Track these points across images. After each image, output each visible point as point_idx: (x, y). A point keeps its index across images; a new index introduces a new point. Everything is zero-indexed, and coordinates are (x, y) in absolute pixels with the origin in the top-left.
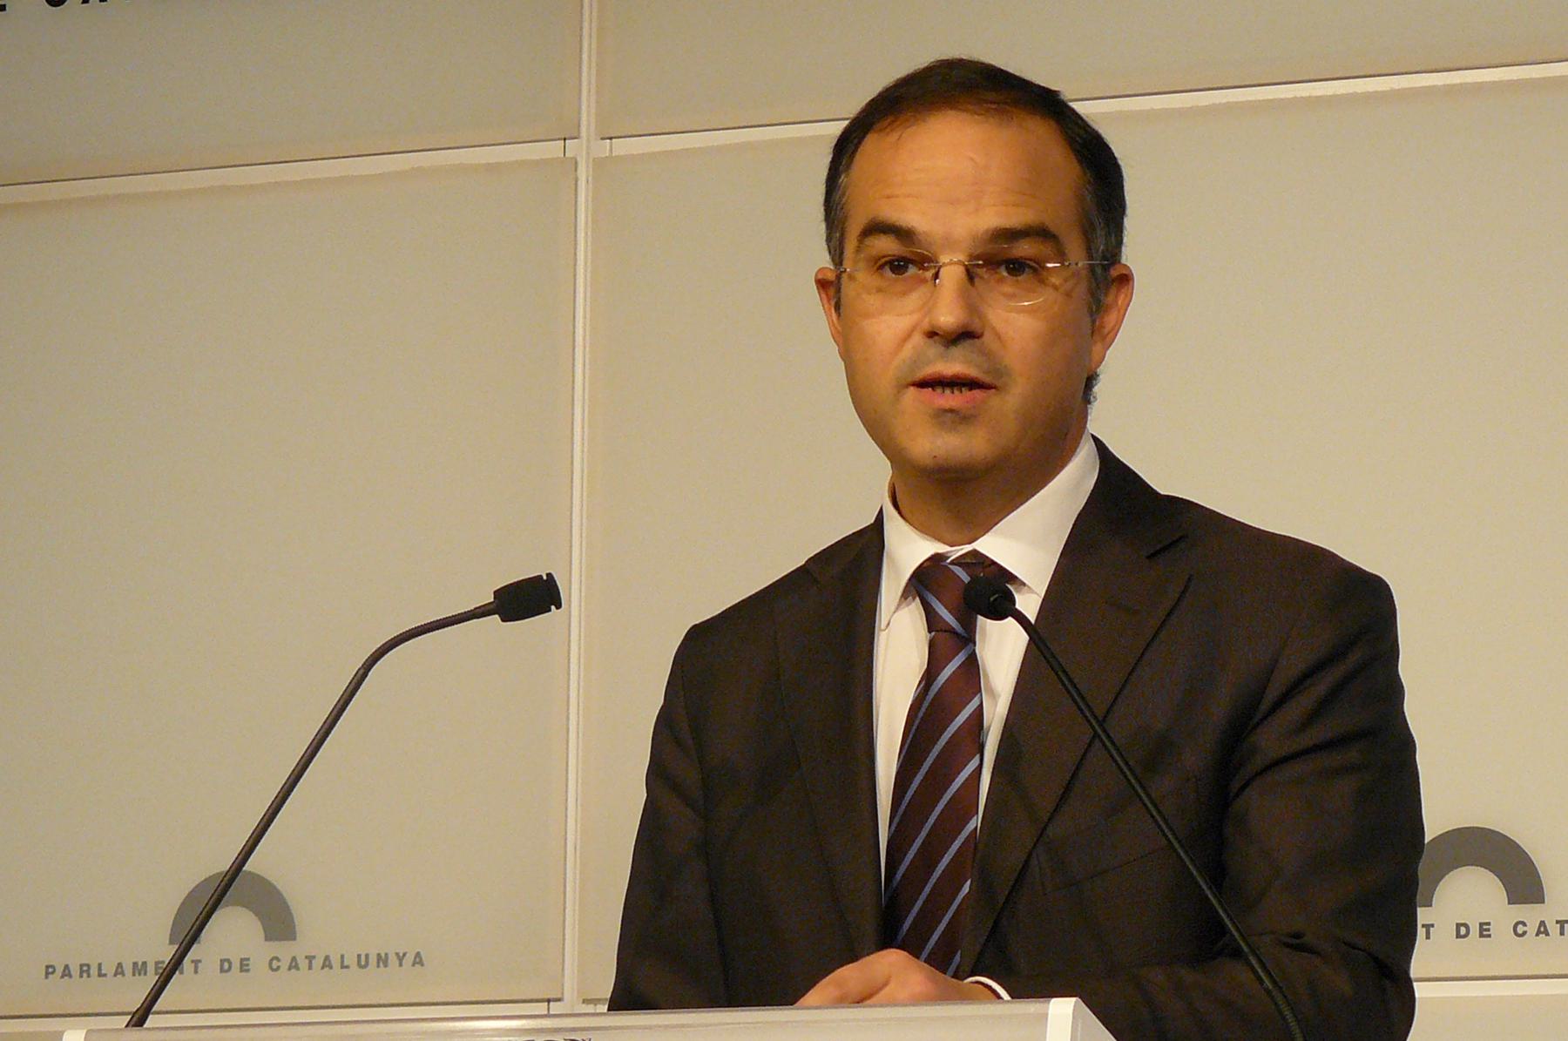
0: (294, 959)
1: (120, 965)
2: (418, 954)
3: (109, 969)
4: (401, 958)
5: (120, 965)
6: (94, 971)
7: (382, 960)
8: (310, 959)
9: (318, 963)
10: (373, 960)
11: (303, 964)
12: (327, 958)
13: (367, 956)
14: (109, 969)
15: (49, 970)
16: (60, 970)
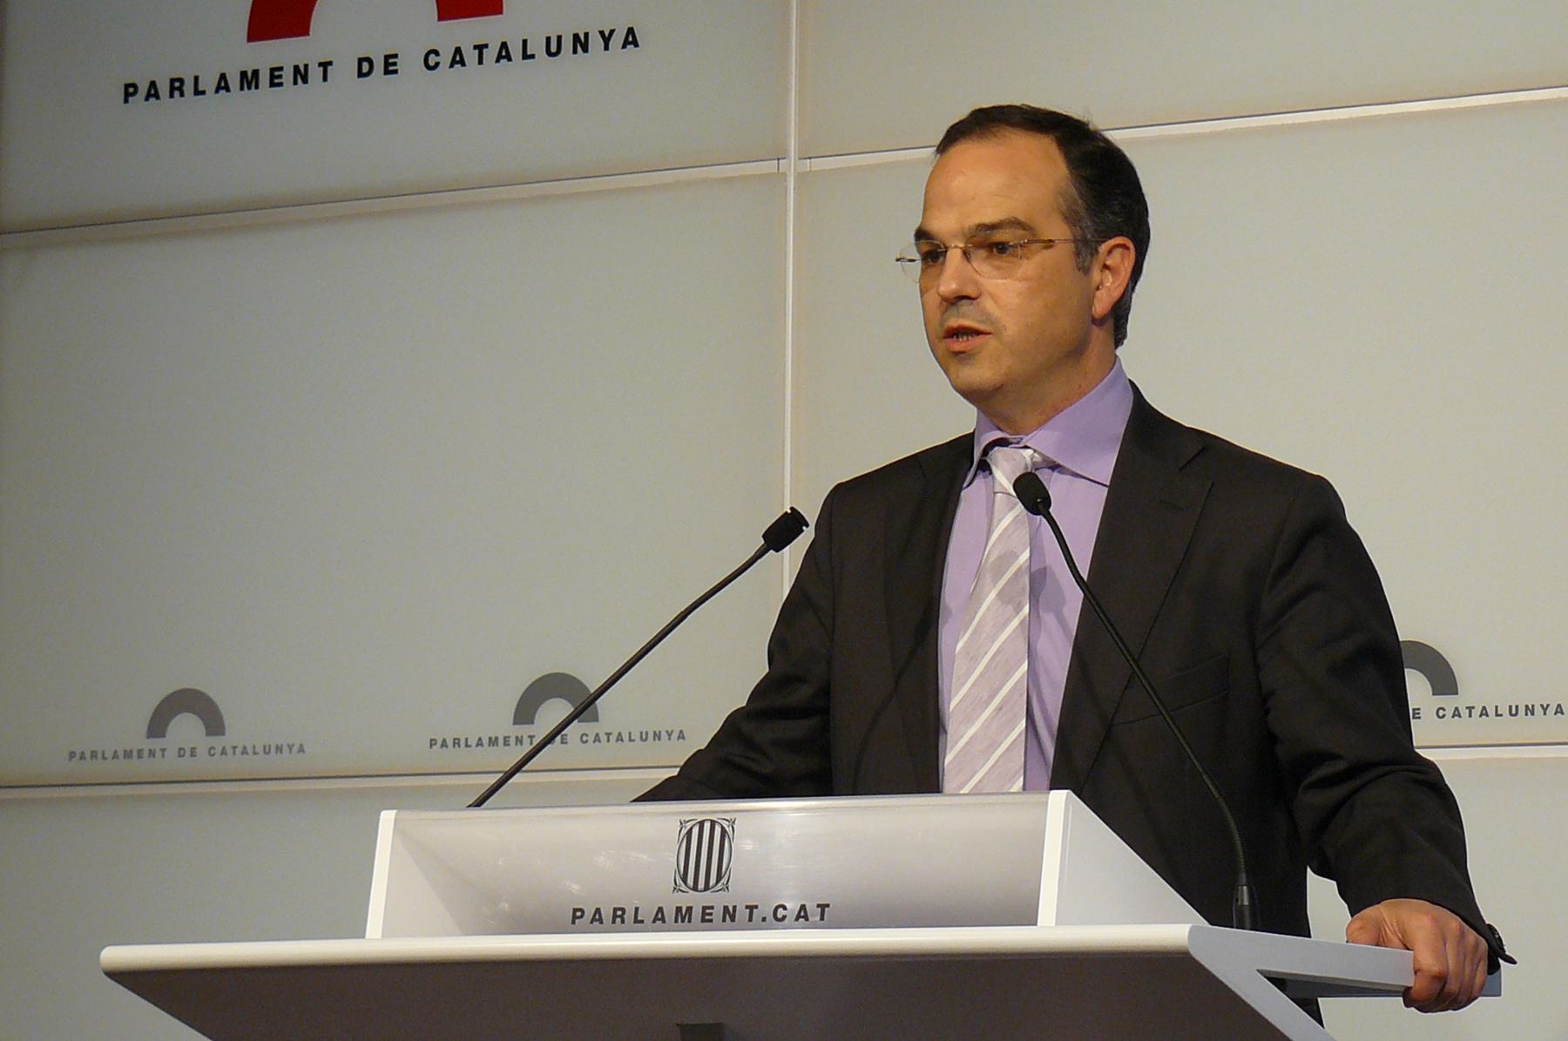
0: (458, 51)
1: (223, 77)
2: (631, 31)
3: (209, 83)
4: (606, 39)
5: (223, 77)
6: (189, 87)
7: (581, 43)
8: (480, 48)
9: (490, 54)
10: (568, 44)
11: (471, 56)
12: (504, 45)
13: (559, 38)
14: (209, 83)
15: (130, 90)
16: (143, 89)
